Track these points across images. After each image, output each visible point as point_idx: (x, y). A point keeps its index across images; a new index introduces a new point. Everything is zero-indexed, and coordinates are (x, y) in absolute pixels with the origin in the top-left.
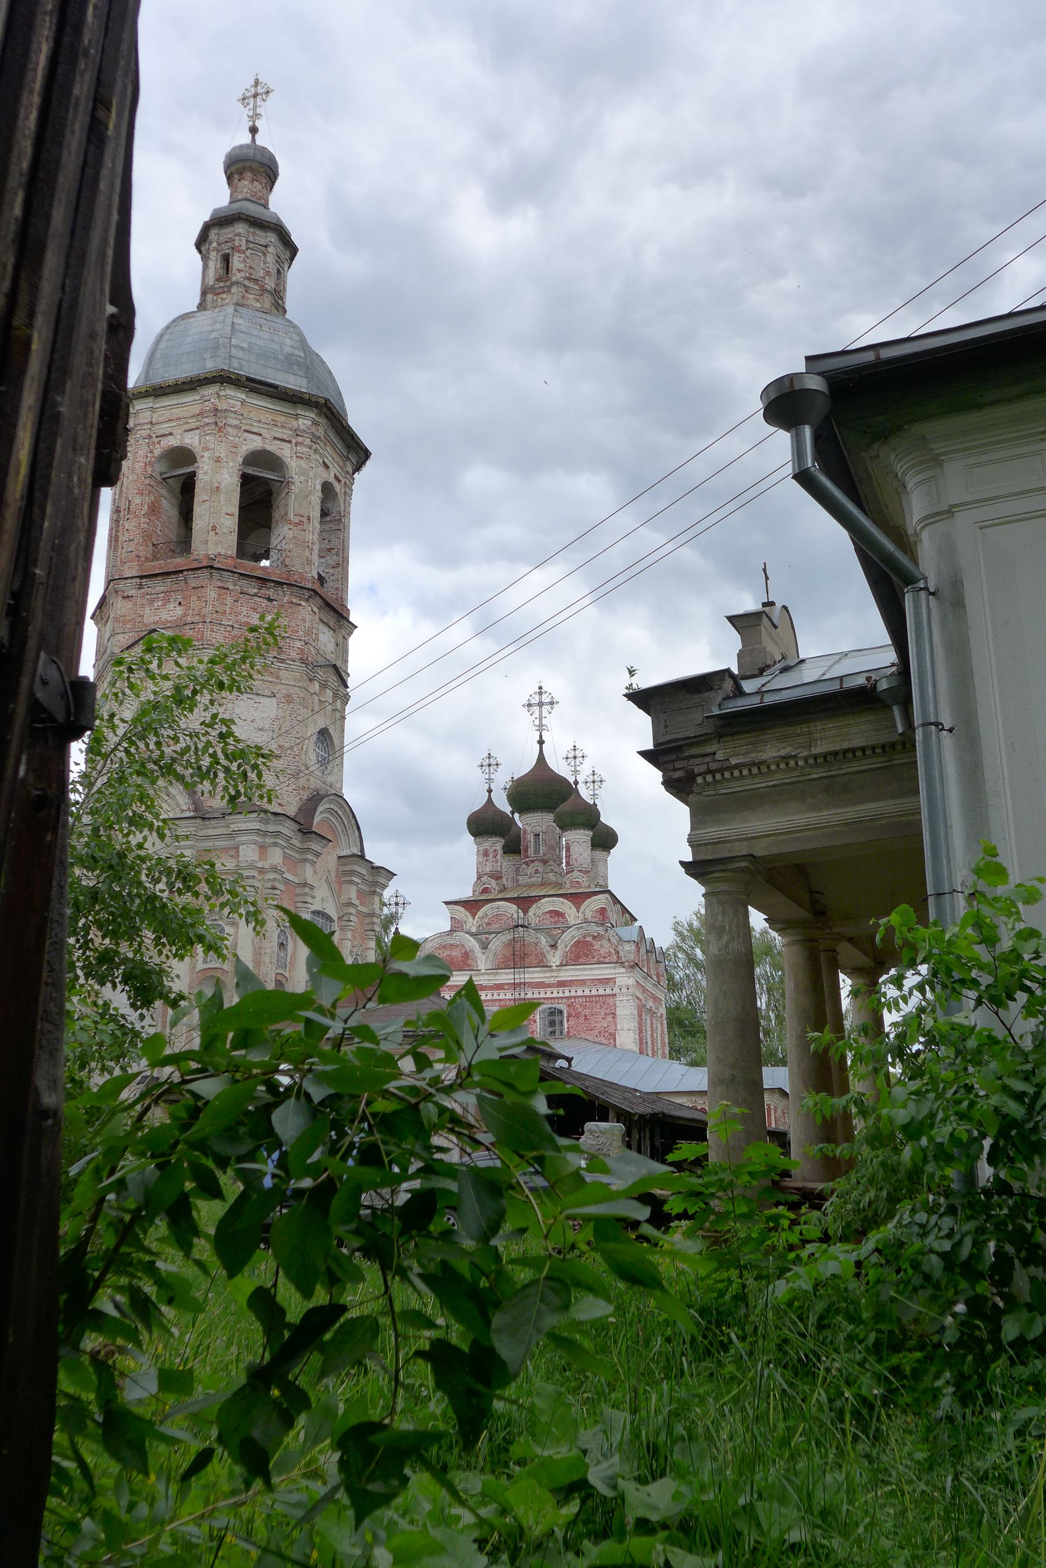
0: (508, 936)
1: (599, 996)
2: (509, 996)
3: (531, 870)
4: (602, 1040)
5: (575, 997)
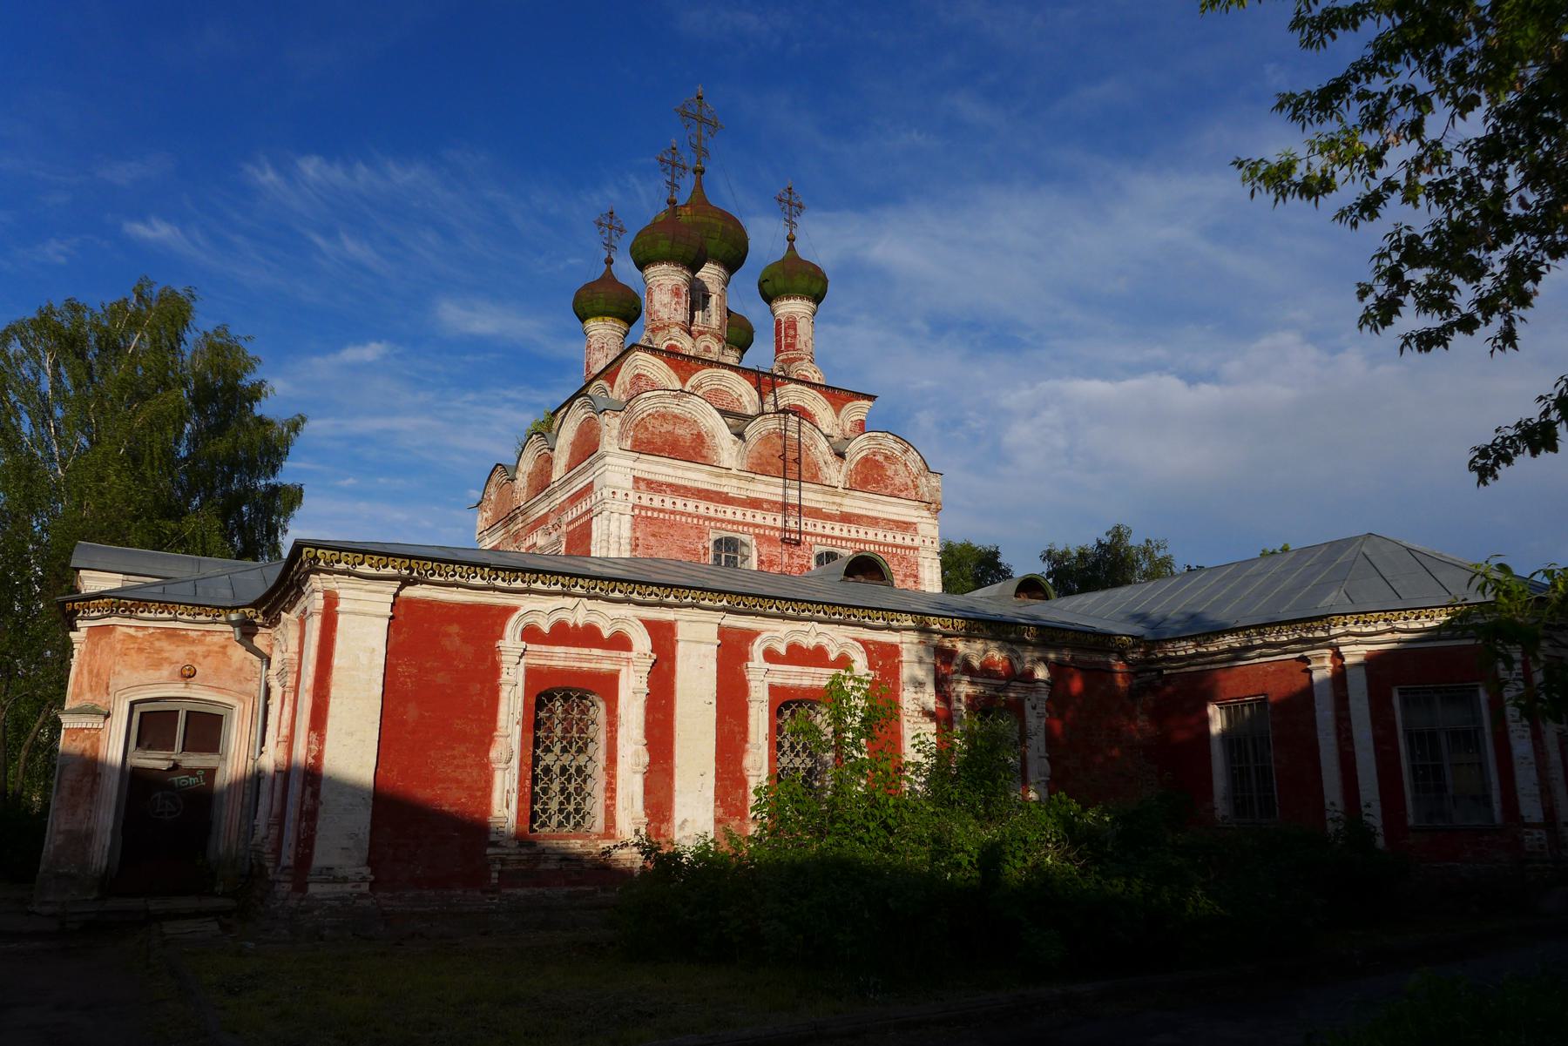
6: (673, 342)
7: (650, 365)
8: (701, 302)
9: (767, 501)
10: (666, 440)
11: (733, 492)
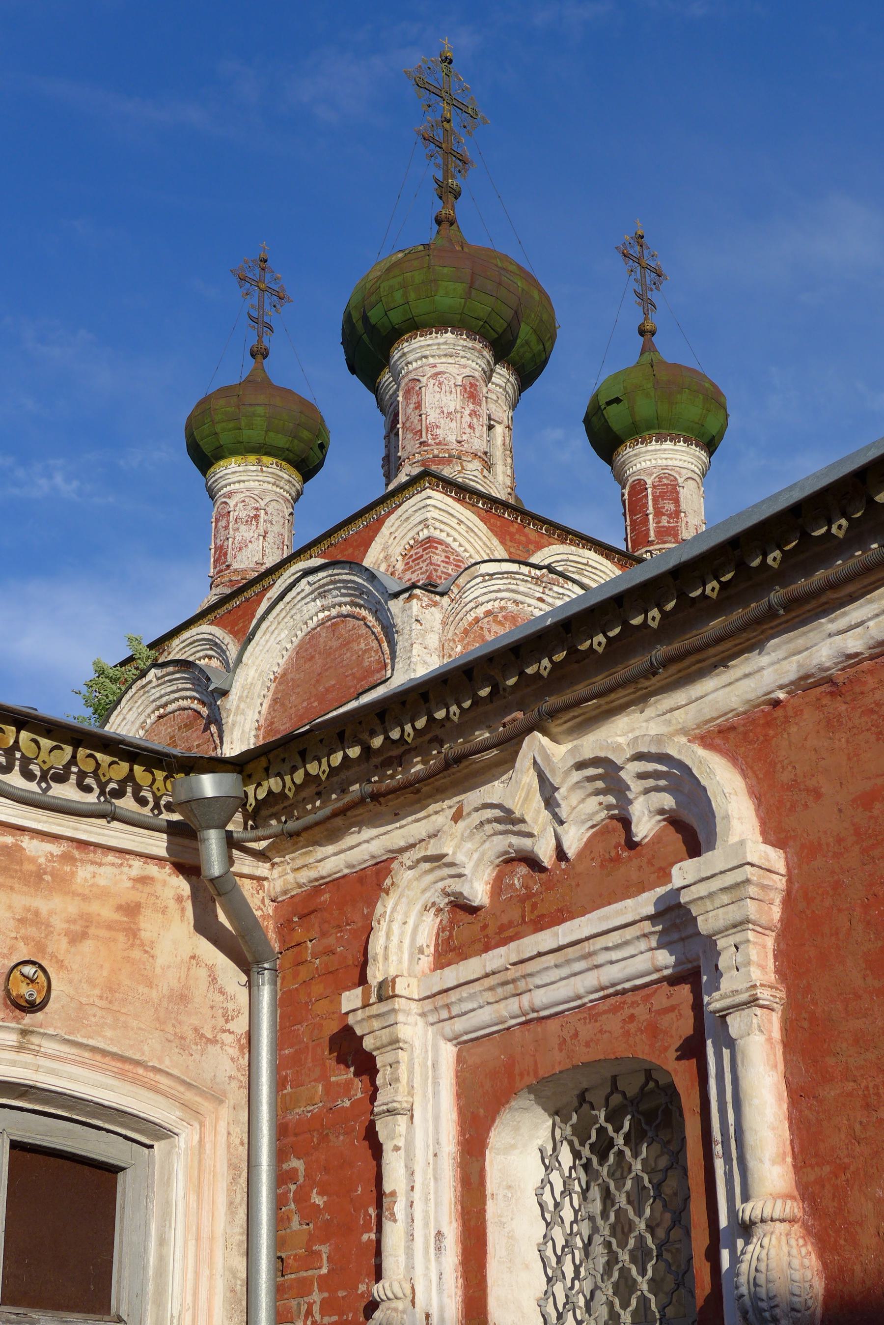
7: (454, 522)
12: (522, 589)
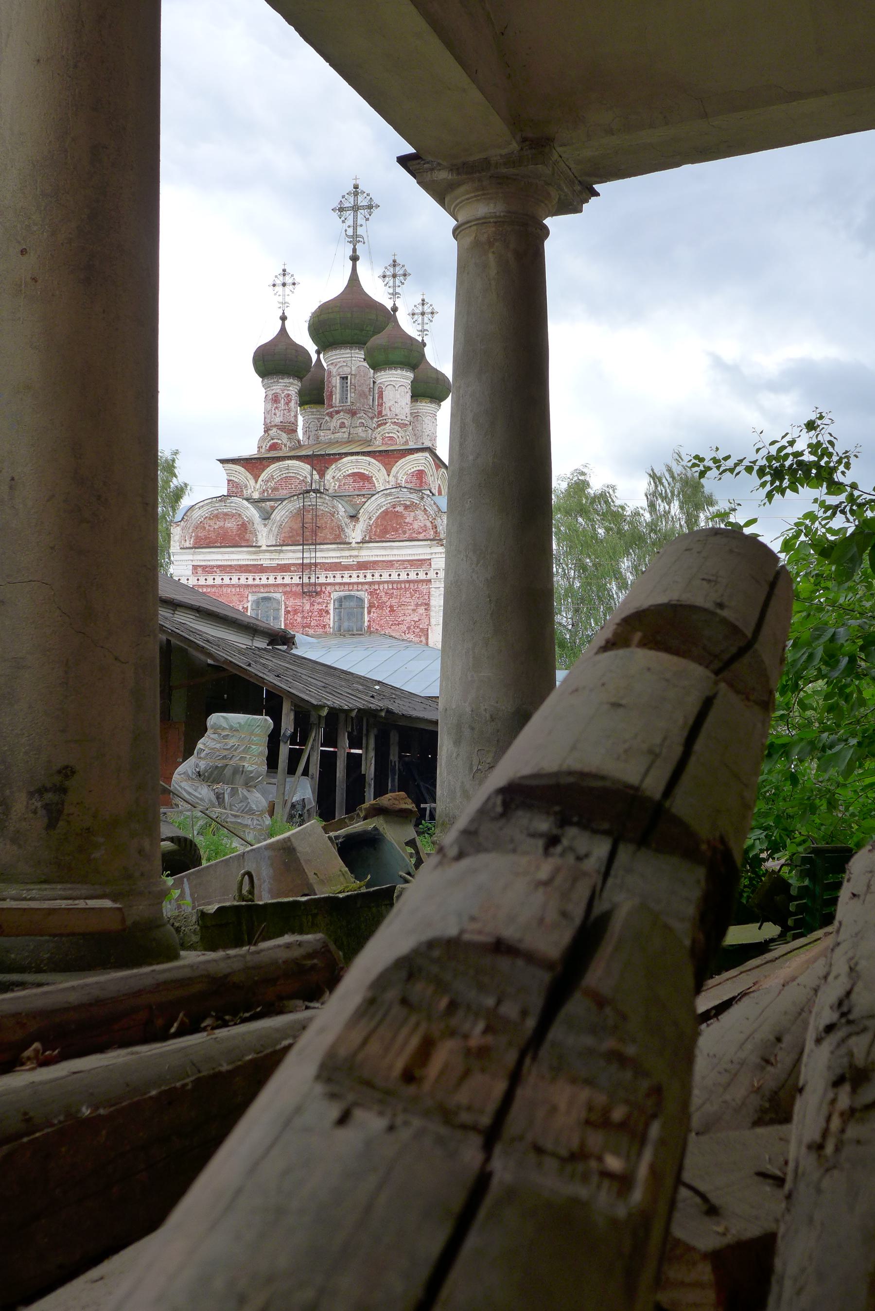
0: (297, 504)
1: (409, 582)
2: (296, 580)
3: (334, 423)
4: (411, 636)
5: (379, 583)
6: (275, 441)
8: (338, 385)
9: (294, 564)
10: (219, 534)
11: (266, 563)
12: (217, 505)
